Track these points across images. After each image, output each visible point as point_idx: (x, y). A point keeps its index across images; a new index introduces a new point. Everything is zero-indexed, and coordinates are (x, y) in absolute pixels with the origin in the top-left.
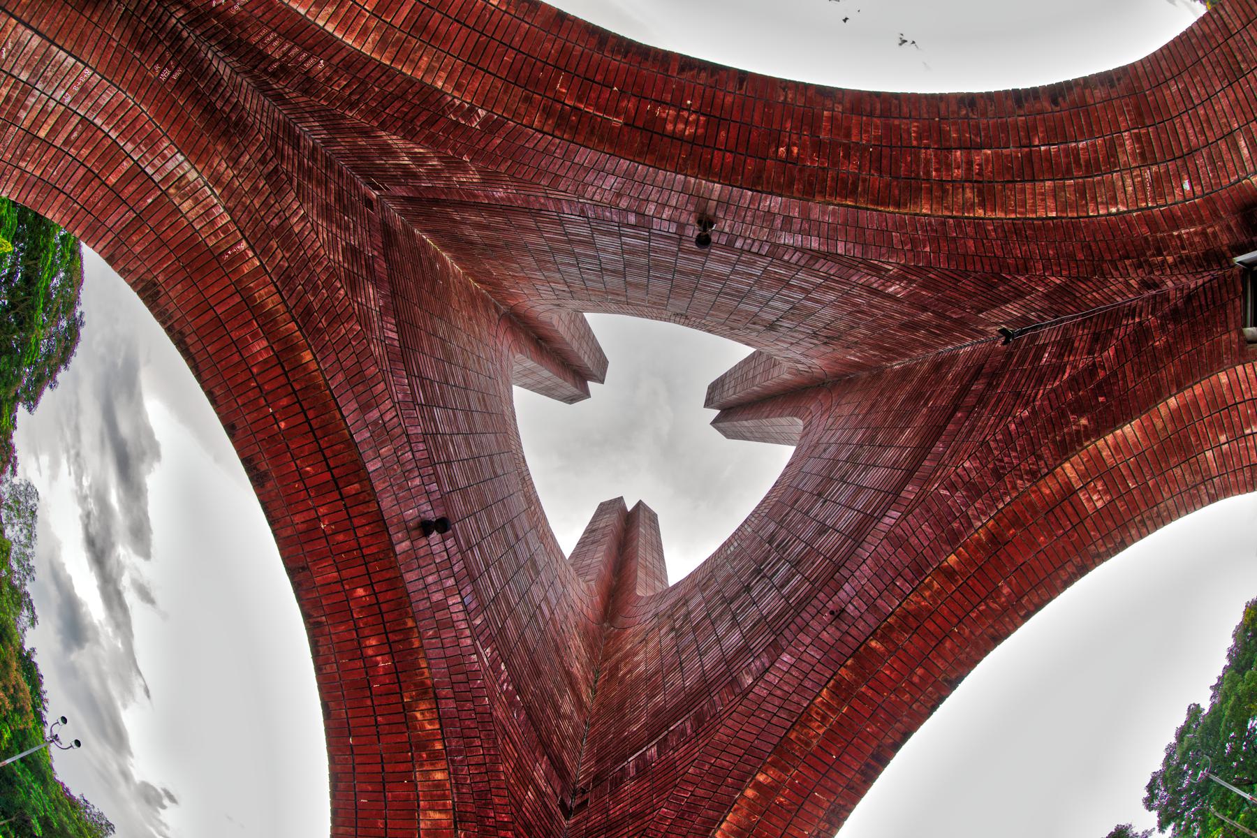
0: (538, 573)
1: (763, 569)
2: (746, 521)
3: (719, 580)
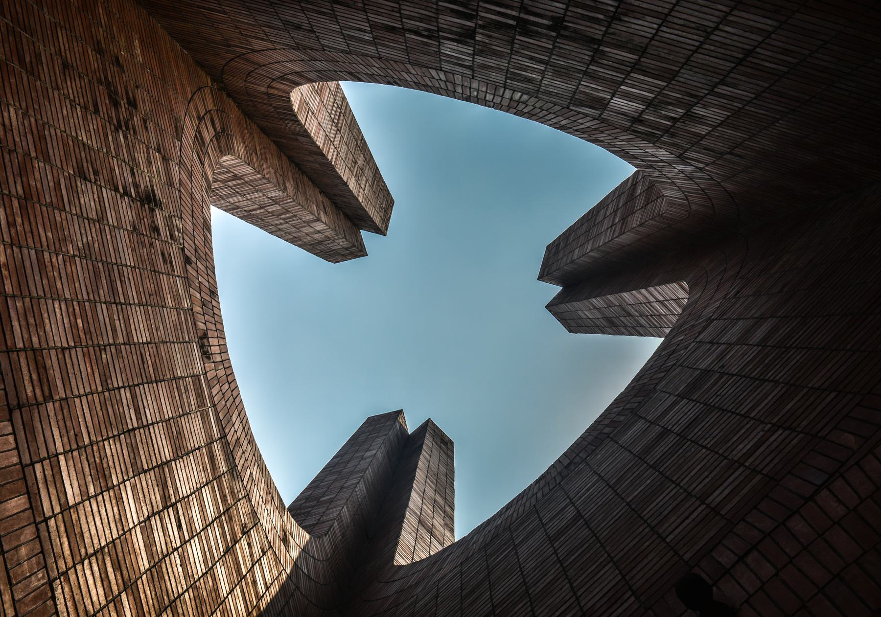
2: (468, 99)
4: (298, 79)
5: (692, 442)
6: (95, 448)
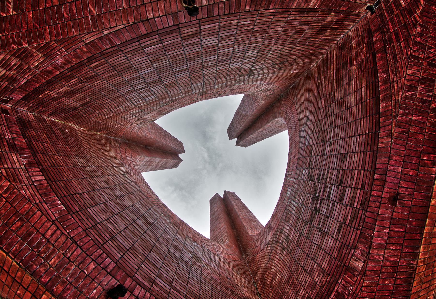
0: (201, 260)
1: (319, 196)
2: (286, 176)
4: (287, 120)
5: (178, 264)
6: (165, 57)
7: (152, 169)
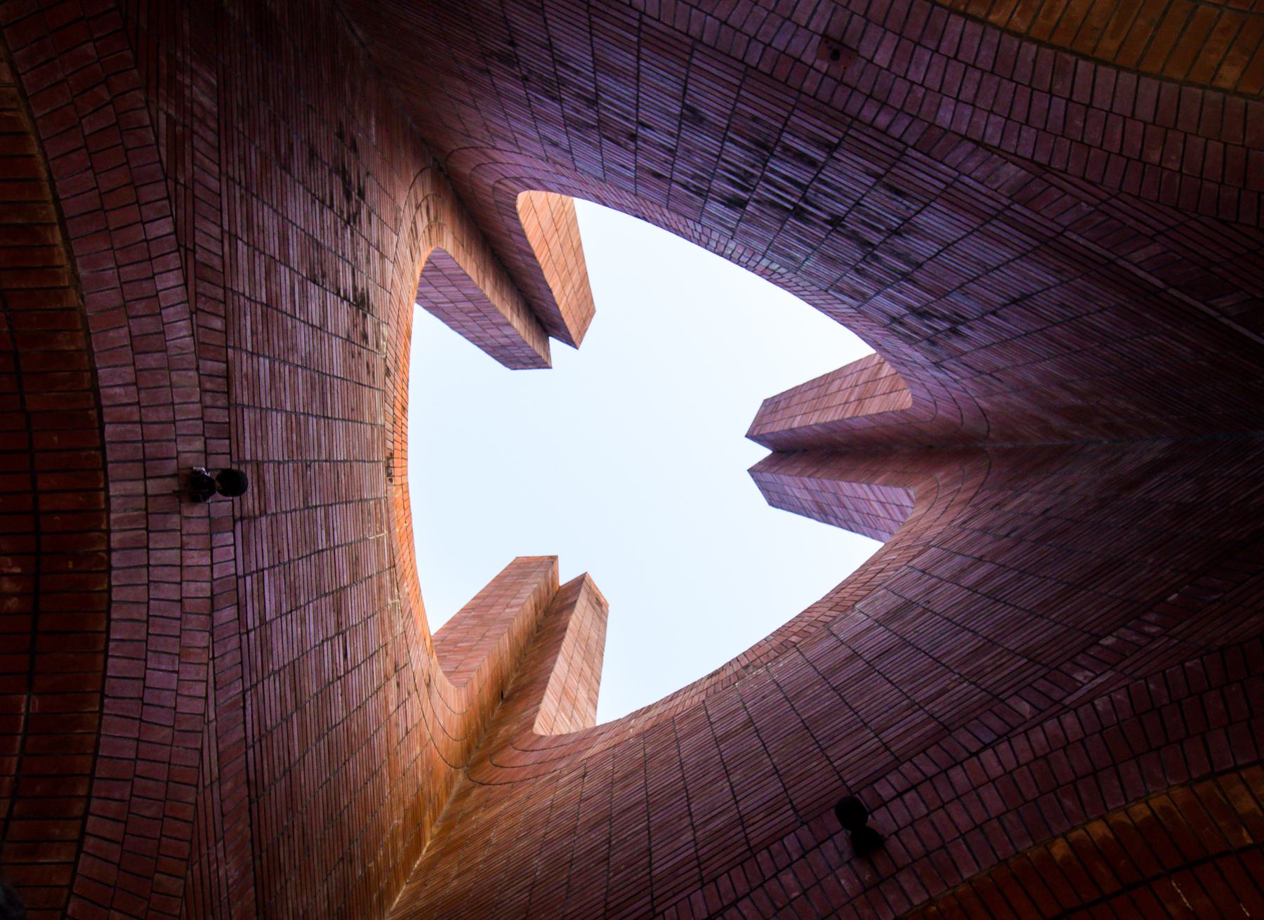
0: (909, 604)
1: (793, 204)
2: (721, 254)
3: (836, 274)
7: (590, 699)
